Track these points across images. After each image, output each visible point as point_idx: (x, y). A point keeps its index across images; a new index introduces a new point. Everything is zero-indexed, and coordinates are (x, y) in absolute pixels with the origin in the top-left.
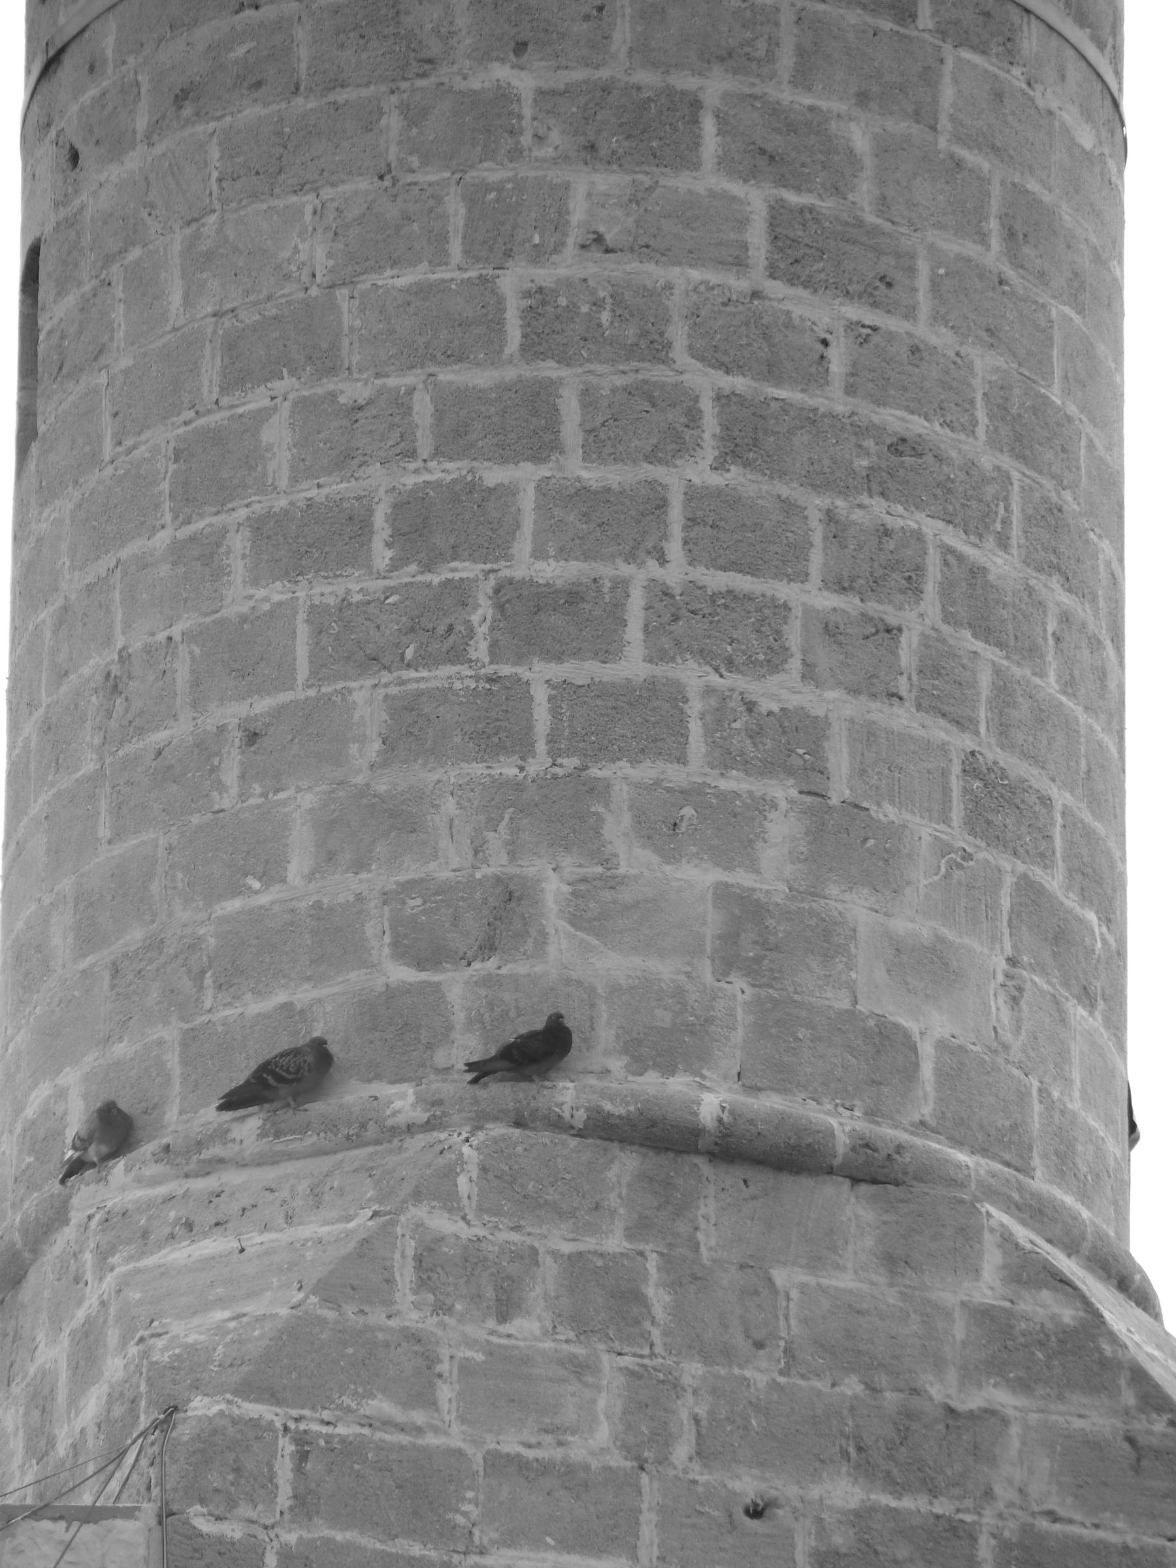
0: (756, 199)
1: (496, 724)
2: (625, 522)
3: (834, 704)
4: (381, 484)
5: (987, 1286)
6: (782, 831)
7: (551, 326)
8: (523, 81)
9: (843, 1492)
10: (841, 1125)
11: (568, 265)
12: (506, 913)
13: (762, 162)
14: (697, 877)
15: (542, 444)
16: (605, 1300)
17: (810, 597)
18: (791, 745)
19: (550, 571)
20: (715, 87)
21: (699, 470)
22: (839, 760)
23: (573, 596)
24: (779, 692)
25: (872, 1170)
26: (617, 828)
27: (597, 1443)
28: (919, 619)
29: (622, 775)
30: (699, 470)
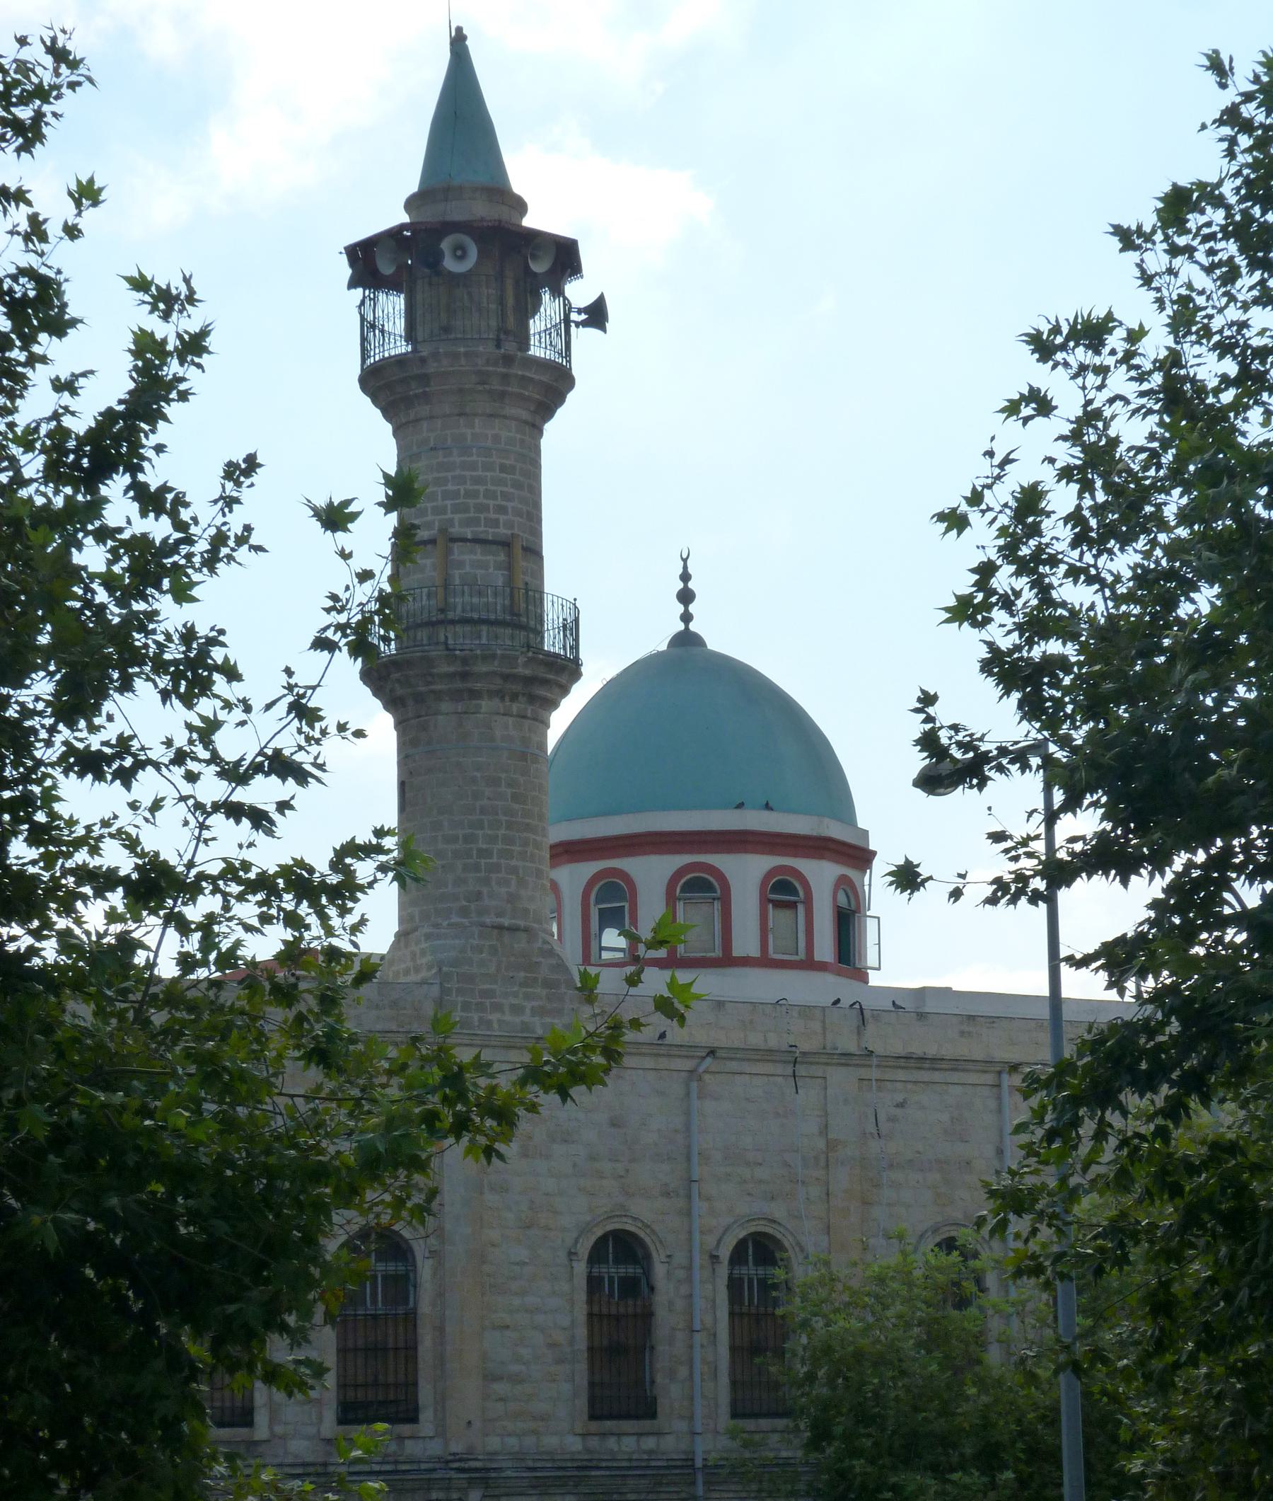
0: (509, 791)
1: (477, 868)
2: (493, 839)
3: (520, 864)
4: (460, 833)
5: (539, 944)
6: (514, 882)
7: (483, 811)
8: (478, 775)
9: (522, 974)
10: (521, 923)
11: (485, 802)
12: (478, 896)
13: (509, 785)
14: (504, 890)
15: (482, 828)
16: (493, 951)
17: (517, 848)
18: (514, 870)
19: (484, 846)
20: (503, 776)
21: (503, 831)
22: (521, 871)
23: (486, 850)
24: (514, 863)
25: (526, 930)
26: (493, 883)
27: (492, 970)
28: (530, 849)
29: (494, 876)
30: (503, 831)
